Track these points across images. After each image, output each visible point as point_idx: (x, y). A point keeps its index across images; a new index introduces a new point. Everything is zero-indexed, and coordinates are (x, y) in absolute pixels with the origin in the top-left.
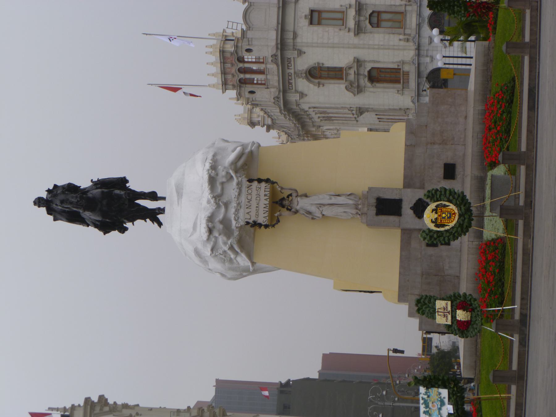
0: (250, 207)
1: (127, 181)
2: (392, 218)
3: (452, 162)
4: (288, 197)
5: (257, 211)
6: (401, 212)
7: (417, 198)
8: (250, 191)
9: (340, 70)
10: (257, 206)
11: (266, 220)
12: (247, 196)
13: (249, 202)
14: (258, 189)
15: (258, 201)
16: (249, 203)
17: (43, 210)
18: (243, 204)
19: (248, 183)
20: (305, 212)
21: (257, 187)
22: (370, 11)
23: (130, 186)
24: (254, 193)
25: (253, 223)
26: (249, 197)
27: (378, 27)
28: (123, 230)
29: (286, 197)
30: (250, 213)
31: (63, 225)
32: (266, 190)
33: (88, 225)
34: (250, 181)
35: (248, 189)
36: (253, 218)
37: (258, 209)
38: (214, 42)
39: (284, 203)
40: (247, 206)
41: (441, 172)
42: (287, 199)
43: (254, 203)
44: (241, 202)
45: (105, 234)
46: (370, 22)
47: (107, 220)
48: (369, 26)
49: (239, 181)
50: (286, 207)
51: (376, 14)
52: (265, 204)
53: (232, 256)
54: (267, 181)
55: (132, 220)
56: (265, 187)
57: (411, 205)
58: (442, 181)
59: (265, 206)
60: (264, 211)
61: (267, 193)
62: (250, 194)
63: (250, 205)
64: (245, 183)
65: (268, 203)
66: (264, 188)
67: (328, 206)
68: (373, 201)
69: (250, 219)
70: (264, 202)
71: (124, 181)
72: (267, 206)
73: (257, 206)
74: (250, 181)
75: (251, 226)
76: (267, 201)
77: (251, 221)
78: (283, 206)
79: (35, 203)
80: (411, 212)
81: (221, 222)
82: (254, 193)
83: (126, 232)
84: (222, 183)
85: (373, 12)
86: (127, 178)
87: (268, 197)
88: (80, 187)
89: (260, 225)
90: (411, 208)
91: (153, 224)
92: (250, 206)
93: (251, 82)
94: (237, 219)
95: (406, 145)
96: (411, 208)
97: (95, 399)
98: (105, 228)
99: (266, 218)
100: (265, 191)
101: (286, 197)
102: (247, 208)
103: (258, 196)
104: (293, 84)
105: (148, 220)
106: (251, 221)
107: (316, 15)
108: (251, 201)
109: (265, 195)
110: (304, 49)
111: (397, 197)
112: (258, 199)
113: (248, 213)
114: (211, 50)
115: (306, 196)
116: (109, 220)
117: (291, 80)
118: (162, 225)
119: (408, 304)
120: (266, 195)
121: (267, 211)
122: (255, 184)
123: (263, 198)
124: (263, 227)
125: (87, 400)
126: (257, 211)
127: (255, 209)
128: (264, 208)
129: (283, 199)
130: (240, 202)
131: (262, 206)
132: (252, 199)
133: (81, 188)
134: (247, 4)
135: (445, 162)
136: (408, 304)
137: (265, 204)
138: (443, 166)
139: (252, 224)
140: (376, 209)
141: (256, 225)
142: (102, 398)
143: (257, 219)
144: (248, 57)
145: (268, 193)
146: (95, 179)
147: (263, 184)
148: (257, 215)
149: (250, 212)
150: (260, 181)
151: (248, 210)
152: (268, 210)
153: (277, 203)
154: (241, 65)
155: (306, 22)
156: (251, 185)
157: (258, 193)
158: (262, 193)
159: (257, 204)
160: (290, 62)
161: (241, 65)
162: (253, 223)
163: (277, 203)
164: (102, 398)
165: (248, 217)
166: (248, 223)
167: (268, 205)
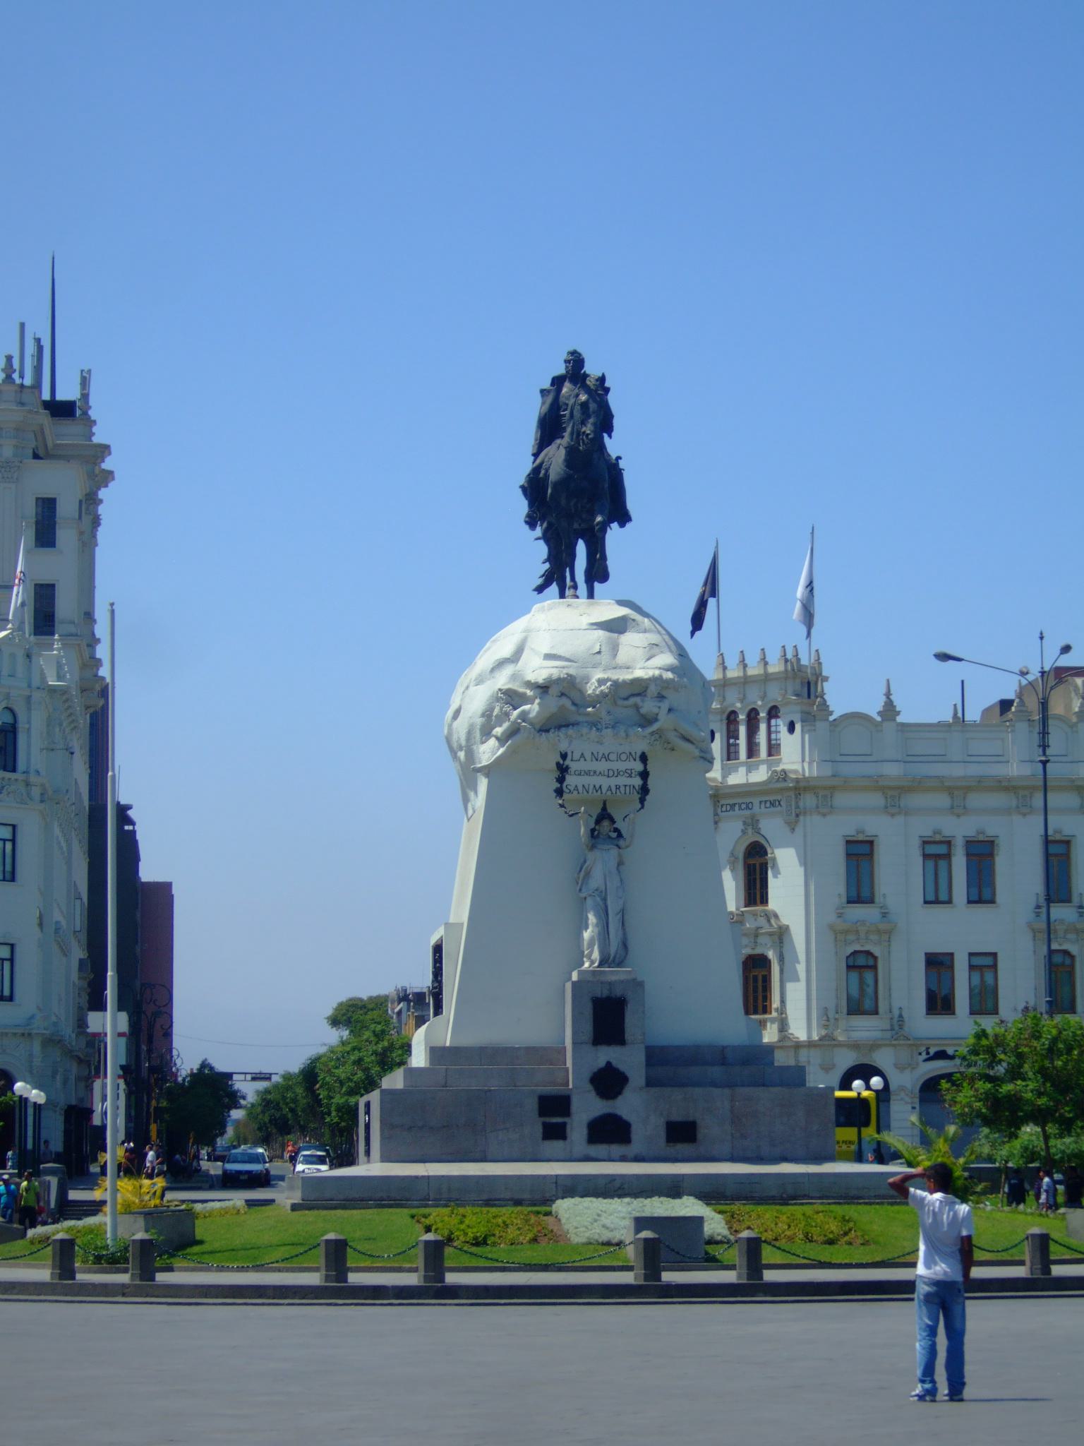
0: (594, 759)
1: (622, 525)
2: (588, 1028)
3: (700, 1136)
4: (616, 830)
5: (588, 773)
6: (601, 1044)
7: (629, 1074)
8: (624, 757)
9: (764, 900)
10: (598, 773)
11: (572, 789)
14: (629, 772)
15: (606, 773)
17: (561, 370)
19: (638, 755)
20: (588, 867)
21: (633, 771)
22: (876, 951)
23: (611, 529)
24: (622, 766)
25: (564, 766)
26: (613, 757)
27: (849, 967)
28: (531, 522)
29: (615, 826)
30: (582, 759)
31: (534, 408)
32: (628, 788)
33: (536, 455)
35: (629, 754)
36: (574, 766)
37: (592, 773)
38: (804, 661)
39: (606, 823)
41: (677, 1116)
42: (612, 830)
43: (602, 766)
45: (522, 487)
46: (855, 952)
47: (549, 491)
48: (850, 950)
50: (597, 827)
51: (871, 962)
52: (600, 787)
53: (498, 731)
54: (644, 790)
55: (546, 537)
56: (634, 787)
57: (615, 1063)
58: (662, 1120)
59: (597, 787)
60: (589, 785)
61: (622, 789)
62: (619, 758)
63: (599, 759)
65: (604, 792)
66: (629, 784)
67: (603, 906)
68: (618, 992)
69: (572, 760)
70: (605, 782)
71: (623, 517)
72: (597, 791)
73: (598, 773)
74: (644, 758)
75: (558, 764)
76: (608, 790)
77: (568, 762)
78: (598, 822)
79: (574, 353)
80: (601, 1063)
83: (527, 527)
84: (637, 707)
85: (875, 958)
86: (628, 525)
88: (610, 436)
89: (561, 780)
90: (609, 1064)
91: (539, 576)
92: (597, 760)
93: (732, 734)
95: (724, 1048)
96: (609, 1064)
97: (107, 465)
98: (535, 487)
99: (574, 790)
100: (625, 786)
101: (615, 826)
102: (592, 753)
103: (616, 774)
104: (731, 813)
105: (547, 566)
106: (568, 762)
107: (866, 848)
109: (618, 787)
110: (799, 830)
111: (628, 1036)
112: (611, 774)
114: (789, 656)
115: (620, 864)
116: (551, 494)
117: (740, 809)
118: (538, 594)
119: (428, 1066)
120: (619, 788)
121: (588, 792)
122: (639, 766)
123: (613, 782)
124: (559, 785)
125: (105, 450)
126: (588, 773)
127: (593, 769)
128: (595, 786)
129: (613, 821)
131: (597, 780)
133: (605, 435)
134: (879, 719)
135: (698, 1121)
136: (428, 1066)
137: (600, 787)
138: (691, 1119)
139: (563, 764)
140: (604, 996)
141: (563, 770)
142: (108, 476)
143: (573, 773)
144: (781, 725)
145: (623, 792)
146: (622, 464)
147: (638, 782)
149: (585, 760)
150: (644, 775)
151: (588, 756)
152: (590, 792)
153: (604, 809)
154: (763, 714)
155: (850, 830)
156: (635, 760)
157: (621, 773)
158: (622, 781)
159: (600, 773)
160: (772, 804)
161: (763, 714)
162: (564, 766)
163: (604, 809)
164: (108, 476)
165: (577, 756)
166: (564, 756)
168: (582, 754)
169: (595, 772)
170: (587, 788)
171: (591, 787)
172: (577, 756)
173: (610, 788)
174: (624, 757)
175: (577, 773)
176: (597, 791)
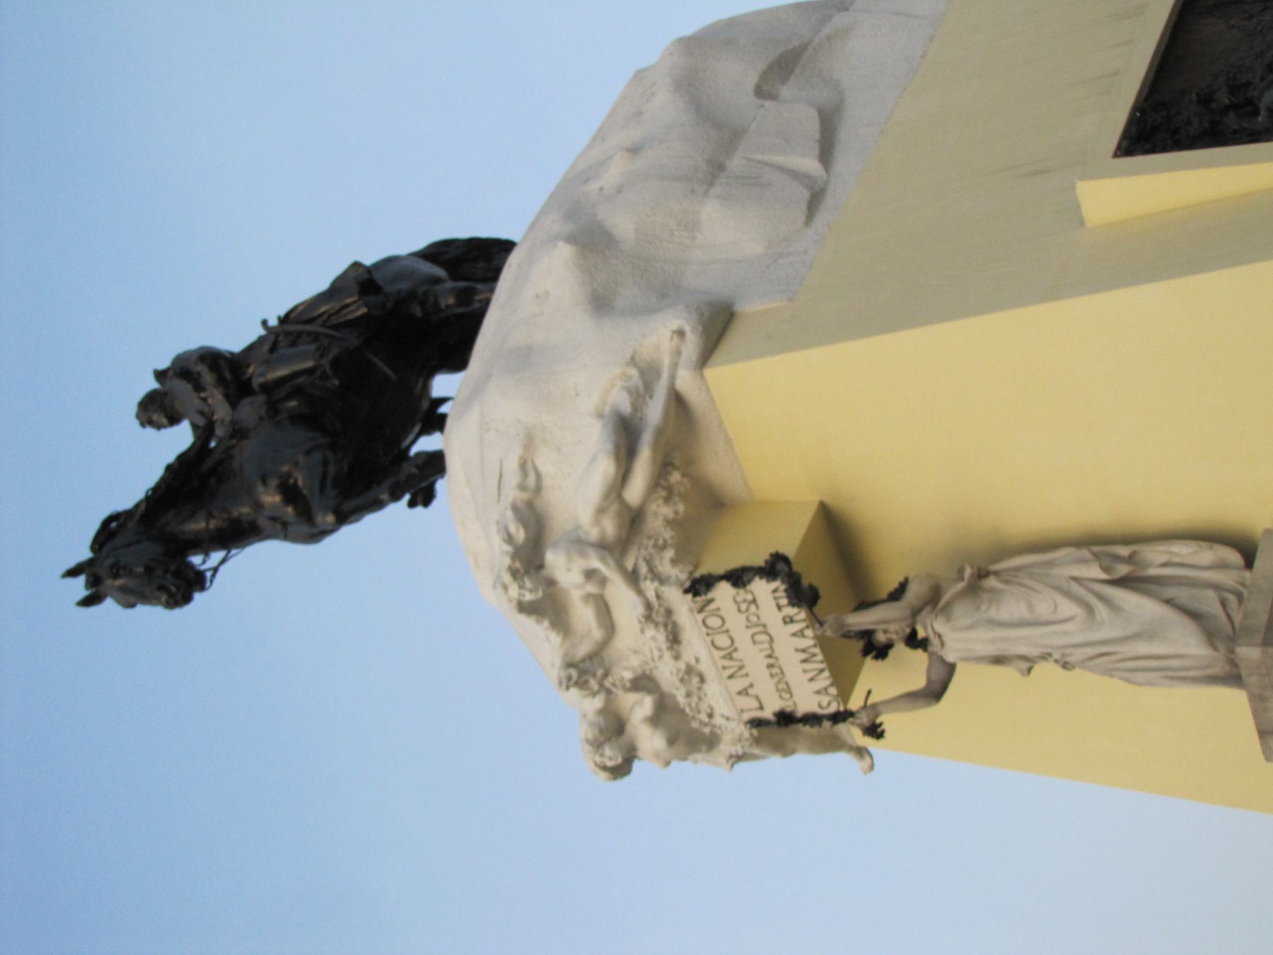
0: (743, 672)
8: (714, 622)
10: (772, 661)
12: (709, 639)
13: (729, 657)
14: (744, 607)
16: (731, 658)
18: (705, 667)
21: (739, 599)
24: (736, 622)
34: (699, 586)
37: (775, 670)
40: (729, 672)
43: (752, 657)
44: (697, 660)
49: (649, 606)
52: (803, 651)
59: (804, 656)
63: (738, 664)
64: (682, 604)
69: (761, 708)
72: (814, 655)
73: (772, 661)
74: (699, 586)
76: (803, 636)
77: (768, 714)
81: (655, 720)
82: (736, 622)
87: (803, 625)
92: (741, 668)
94: (706, 719)
99: (827, 694)
108: (736, 650)
113: (744, 692)
122: (723, 592)
130: (693, 662)
132: (737, 644)
137: (803, 651)
143: (790, 703)
148: (785, 689)
150: (738, 578)
159: (770, 656)
167: (817, 650)
168: (739, 693)
169: (770, 666)
170: (815, 673)
171: (807, 666)
172: (750, 703)
173: (800, 634)
174: (714, 622)
175: (787, 696)
176: (814, 655)
